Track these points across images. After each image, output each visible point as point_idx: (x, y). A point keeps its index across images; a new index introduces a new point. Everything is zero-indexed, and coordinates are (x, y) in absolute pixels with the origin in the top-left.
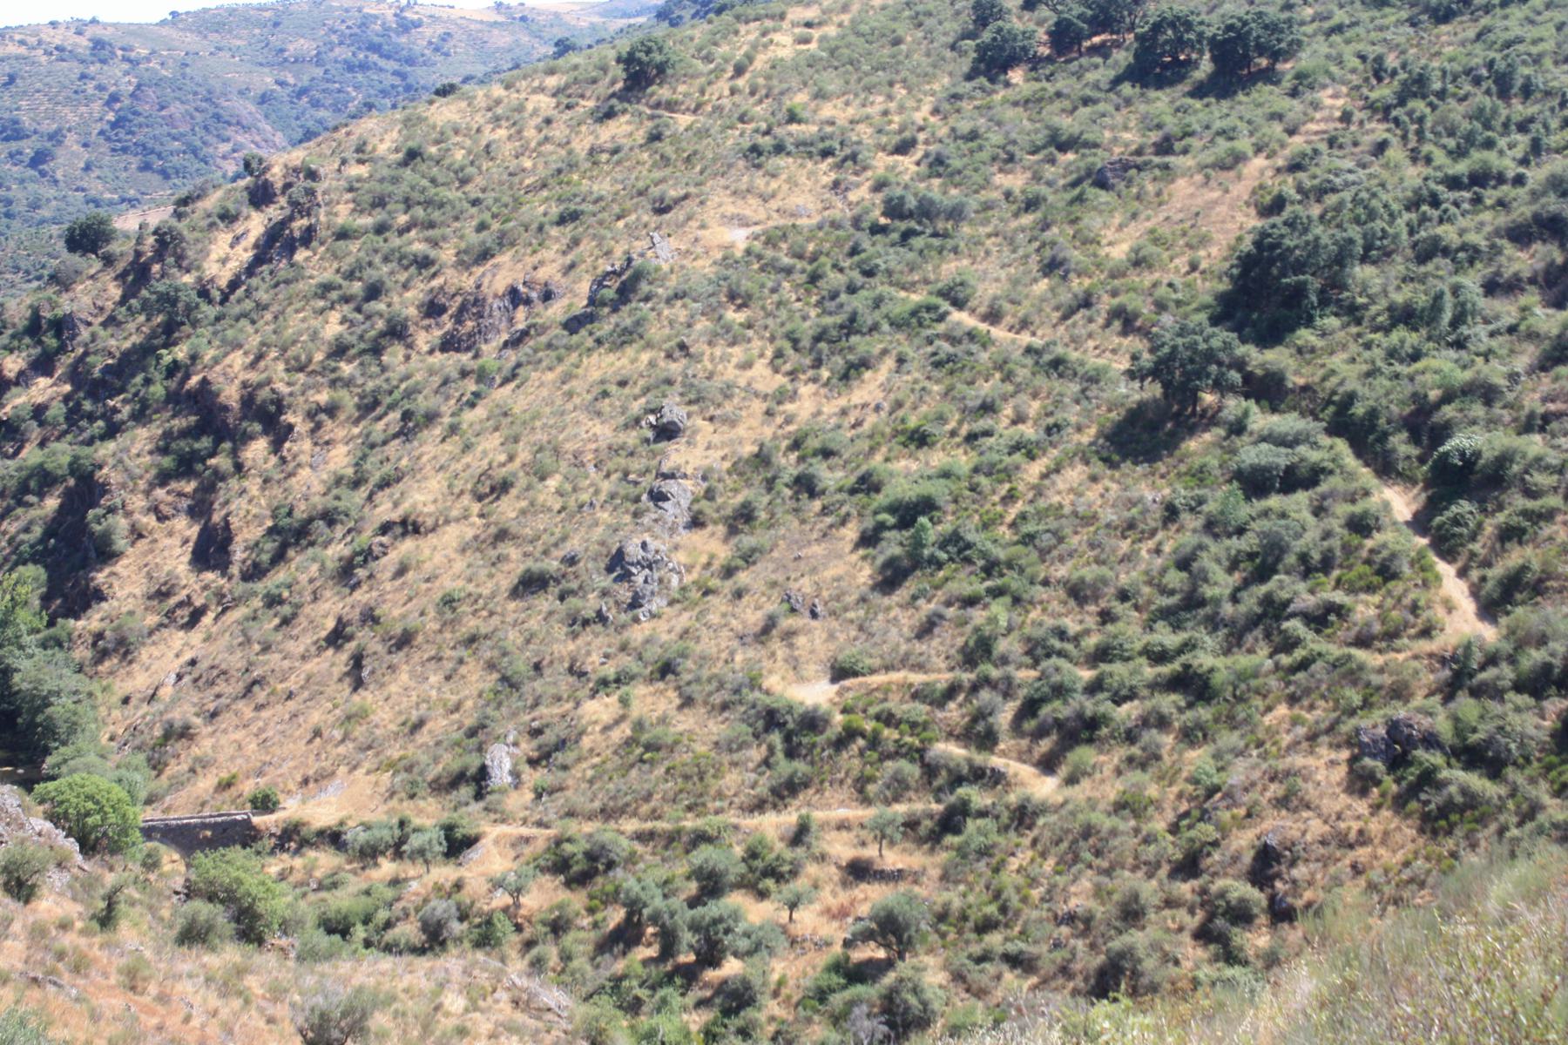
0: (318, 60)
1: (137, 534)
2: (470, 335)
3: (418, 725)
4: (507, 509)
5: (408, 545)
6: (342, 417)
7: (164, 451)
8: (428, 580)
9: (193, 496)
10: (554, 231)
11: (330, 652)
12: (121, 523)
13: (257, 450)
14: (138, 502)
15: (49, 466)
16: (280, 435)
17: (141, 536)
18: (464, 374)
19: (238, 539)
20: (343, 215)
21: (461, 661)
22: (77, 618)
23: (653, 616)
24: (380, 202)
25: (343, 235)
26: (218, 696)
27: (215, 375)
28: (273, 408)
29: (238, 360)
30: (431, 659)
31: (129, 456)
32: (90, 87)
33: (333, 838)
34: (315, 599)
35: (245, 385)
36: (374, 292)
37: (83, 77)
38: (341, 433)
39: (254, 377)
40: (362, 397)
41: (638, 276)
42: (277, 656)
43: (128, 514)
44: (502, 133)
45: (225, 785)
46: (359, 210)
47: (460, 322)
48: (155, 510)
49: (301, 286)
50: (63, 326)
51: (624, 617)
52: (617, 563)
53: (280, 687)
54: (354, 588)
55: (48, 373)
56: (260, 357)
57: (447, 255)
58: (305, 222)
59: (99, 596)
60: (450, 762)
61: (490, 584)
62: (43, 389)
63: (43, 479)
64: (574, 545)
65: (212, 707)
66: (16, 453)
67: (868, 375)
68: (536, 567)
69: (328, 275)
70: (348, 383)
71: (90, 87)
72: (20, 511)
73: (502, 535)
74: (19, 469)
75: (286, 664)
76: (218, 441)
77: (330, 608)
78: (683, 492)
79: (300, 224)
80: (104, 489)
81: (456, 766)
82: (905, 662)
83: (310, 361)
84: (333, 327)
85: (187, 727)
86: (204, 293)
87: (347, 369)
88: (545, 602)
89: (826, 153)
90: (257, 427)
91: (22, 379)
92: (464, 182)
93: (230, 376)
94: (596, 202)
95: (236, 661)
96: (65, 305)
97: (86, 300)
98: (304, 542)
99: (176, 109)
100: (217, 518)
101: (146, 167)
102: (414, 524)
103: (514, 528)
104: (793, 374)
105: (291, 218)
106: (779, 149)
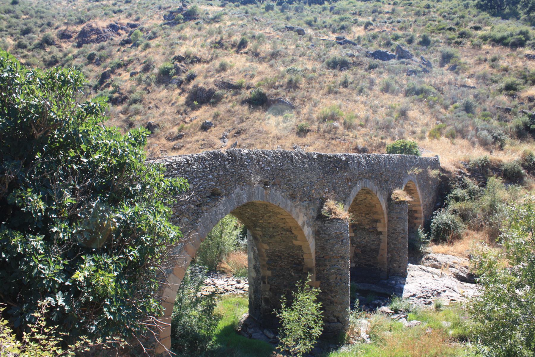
10: (114, 15)
11: (204, 108)
34: (149, 92)
40: (44, 61)
73: (274, 55)
87: (30, 53)
102: (196, 58)
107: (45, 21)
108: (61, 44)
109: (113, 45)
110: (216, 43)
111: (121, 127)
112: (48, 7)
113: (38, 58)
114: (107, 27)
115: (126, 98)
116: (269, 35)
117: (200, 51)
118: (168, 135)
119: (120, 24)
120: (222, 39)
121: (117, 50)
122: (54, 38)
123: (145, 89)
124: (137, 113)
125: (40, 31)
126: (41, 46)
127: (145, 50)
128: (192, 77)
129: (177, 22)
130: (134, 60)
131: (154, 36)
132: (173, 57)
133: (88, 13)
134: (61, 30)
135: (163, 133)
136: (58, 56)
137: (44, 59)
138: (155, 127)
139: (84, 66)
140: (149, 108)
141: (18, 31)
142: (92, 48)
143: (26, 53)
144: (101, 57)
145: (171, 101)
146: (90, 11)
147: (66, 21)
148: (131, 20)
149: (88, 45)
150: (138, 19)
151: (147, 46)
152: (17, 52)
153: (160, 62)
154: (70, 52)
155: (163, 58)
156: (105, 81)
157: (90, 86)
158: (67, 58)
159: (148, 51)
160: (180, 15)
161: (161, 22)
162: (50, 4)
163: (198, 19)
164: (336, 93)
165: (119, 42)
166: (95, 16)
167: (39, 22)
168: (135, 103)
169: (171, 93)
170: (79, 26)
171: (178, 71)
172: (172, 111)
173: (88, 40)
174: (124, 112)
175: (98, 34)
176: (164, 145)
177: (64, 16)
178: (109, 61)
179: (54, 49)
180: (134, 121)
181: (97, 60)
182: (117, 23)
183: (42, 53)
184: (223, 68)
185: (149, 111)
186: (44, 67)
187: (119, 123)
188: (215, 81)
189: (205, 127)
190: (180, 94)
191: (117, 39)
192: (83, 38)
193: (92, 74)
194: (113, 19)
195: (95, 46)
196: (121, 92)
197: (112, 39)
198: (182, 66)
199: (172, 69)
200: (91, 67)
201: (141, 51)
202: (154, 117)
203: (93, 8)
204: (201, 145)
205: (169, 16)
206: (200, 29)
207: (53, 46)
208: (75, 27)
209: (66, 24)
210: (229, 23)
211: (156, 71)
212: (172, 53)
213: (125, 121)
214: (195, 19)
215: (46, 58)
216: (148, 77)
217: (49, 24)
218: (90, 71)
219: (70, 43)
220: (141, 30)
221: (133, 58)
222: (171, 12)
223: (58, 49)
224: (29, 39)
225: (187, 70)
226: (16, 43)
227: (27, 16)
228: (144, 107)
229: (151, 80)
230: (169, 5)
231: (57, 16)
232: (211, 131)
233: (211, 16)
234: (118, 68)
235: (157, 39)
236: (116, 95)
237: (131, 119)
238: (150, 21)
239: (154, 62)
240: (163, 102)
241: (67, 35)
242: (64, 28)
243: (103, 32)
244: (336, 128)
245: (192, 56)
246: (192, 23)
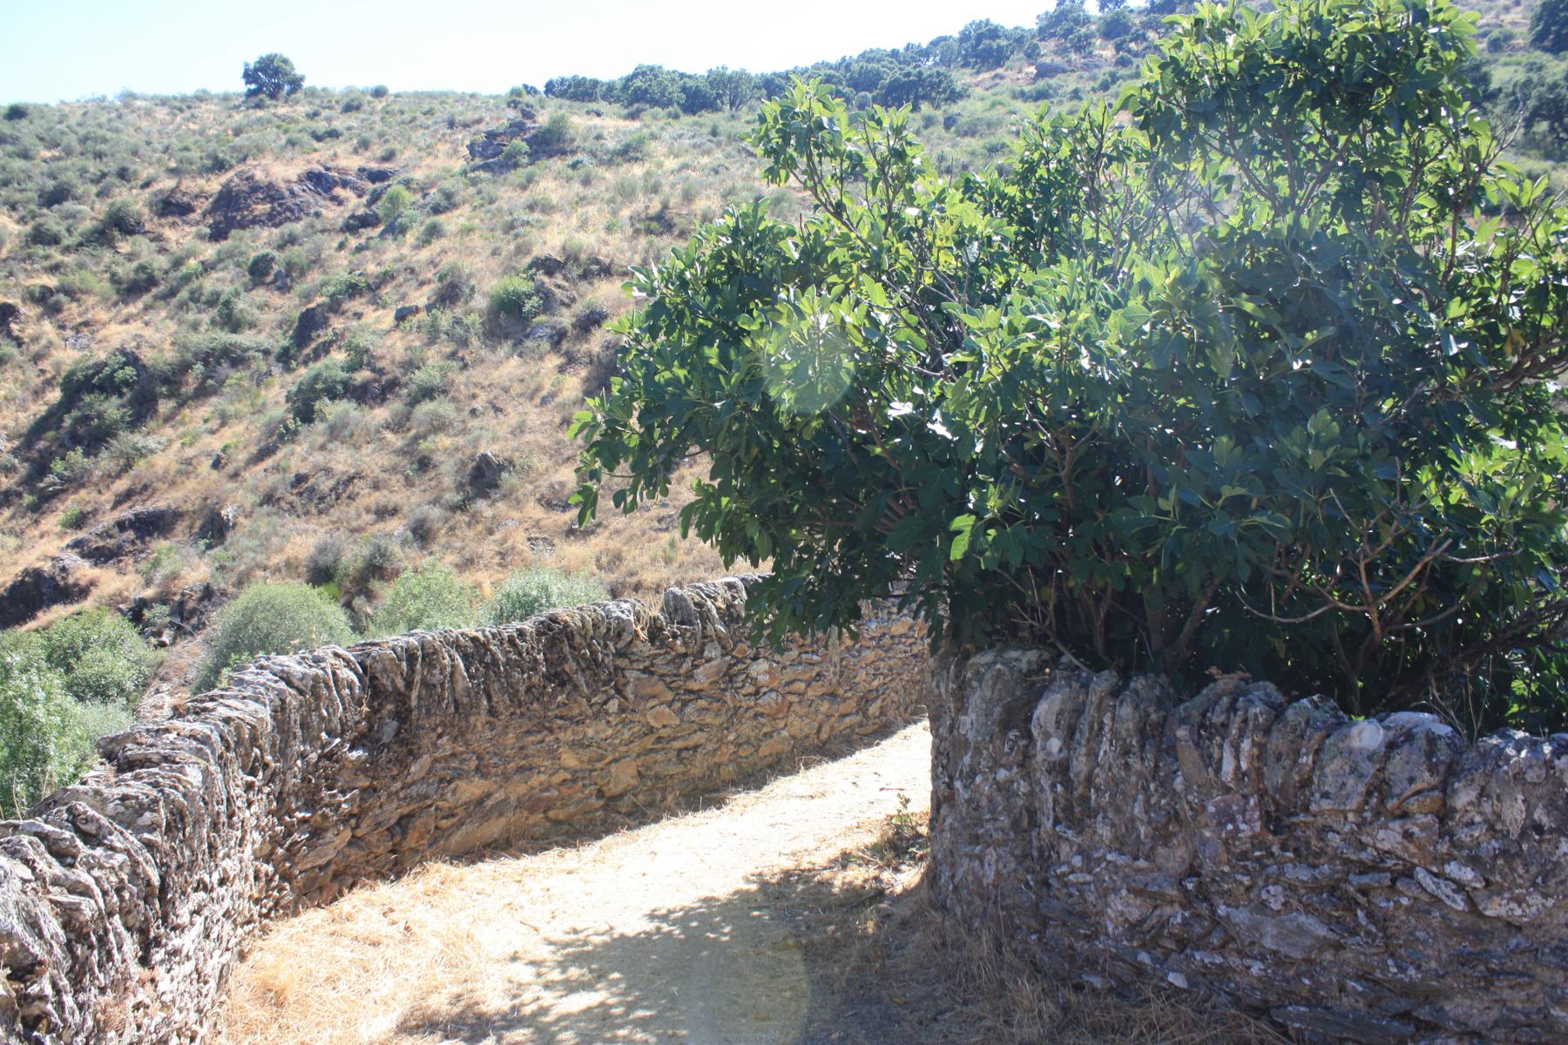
10: (316, 145)
34: (465, 367)
38: (103, 315)
40: (114, 279)
87: (69, 259)
102: (597, 262)
107: (111, 166)
108: (161, 230)
109: (323, 231)
110: (651, 219)
111: (394, 470)
112: (117, 124)
113: (95, 274)
114: (300, 181)
115: (393, 384)
118: (544, 490)
119: (338, 170)
120: (665, 207)
121: (335, 245)
122: (140, 214)
123: (453, 355)
124: (439, 426)
125: (99, 195)
127: (429, 242)
128: (591, 321)
129: (510, 163)
130: (398, 271)
131: (448, 203)
132: (528, 260)
133: (238, 141)
134: (161, 191)
135: (530, 487)
136: (155, 265)
137: (114, 275)
138: (501, 468)
139: (243, 294)
140: (473, 412)
141: (30, 194)
142: (258, 241)
143: (57, 256)
144: (290, 266)
145: (538, 389)
146: (244, 136)
147: (173, 164)
148: (369, 160)
149: (247, 234)
150: (389, 156)
151: (434, 232)
152: (30, 256)
153: (489, 281)
154: (191, 254)
155: (494, 263)
156: (314, 335)
157: (266, 352)
158: (184, 270)
159: (437, 245)
160: (519, 143)
161: (459, 165)
162: (120, 117)
163: (573, 152)
165: (340, 222)
166: (260, 150)
167: (93, 167)
168: (432, 399)
169: (533, 368)
170: (213, 177)
171: (548, 302)
172: (546, 419)
173: (243, 217)
174: (397, 425)
175: (272, 199)
176: (538, 522)
177: (166, 150)
178: (314, 277)
179: (143, 245)
180: (432, 451)
181: (278, 274)
182: (328, 169)
183: (107, 256)
185: (476, 423)
186: (115, 297)
187: (386, 460)
190: (561, 369)
191: (334, 215)
192: (229, 213)
193: (268, 317)
194: (316, 156)
196: (380, 364)
197: (317, 215)
198: (559, 287)
199: (529, 296)
200: (260, 294)
201: (417, 247)
202: (495, 440)
203: (250, 125)
204: (660, 520)
205: (485, 146)
206: (586, 182)
207: (138, 237)
208: (201, 182)
209: (173, 172)
210: (671, 164)
211: (480, 302)
212: (521, 250)
213: (402, 452)
214: (564, 153)
215: (120, 271)
216: (458, 322)
217: (123, 174)
218: (261, 308)
219: (187, 229)
220: (407, 184)
221: (398, 266)
222: (491, 135)
223: (153, 245)
225: (573, 300)
226: (28, 228)
228: (459, 410)
229: (467, 331)
230: (476, 116)
231: (144, 150)
232: (683, 477)
233: (611, 144)
234: (352, 296)
235: (457, 212)
236: (363, 375)
237: (423, 445)
238: (429, 160)
239: (470, 276)
240: (513, 393)
241: (178, 205)
242: (167, 183)
243: (287, 194)
245: (583, 257)
246: (557, 164)
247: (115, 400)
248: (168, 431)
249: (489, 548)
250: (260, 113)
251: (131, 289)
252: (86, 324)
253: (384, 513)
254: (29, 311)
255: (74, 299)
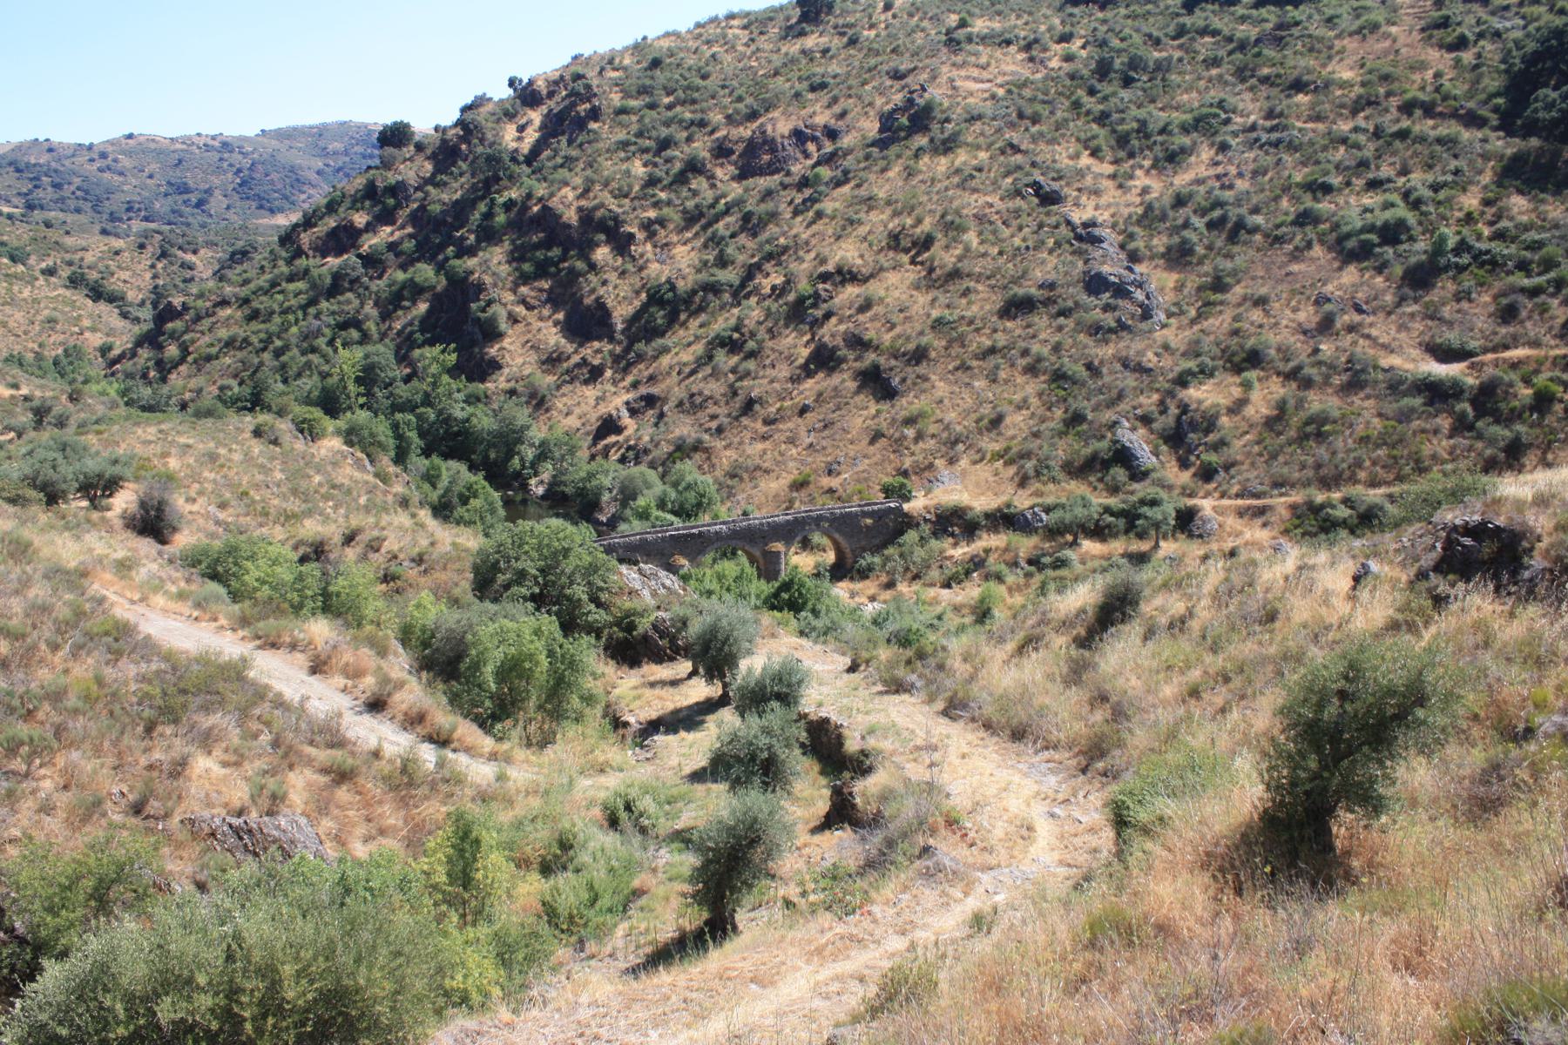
0: (346, 153)
1: (514, 319)
2: (770, 164)
3: (996, 422)
4: (944, 257)
5: (851, 291)
6: (672, 226)
7: (522, 259)
8: (901, 311)
9: (550, 291)
10: (810, 96)
11: (821, 375)
12: (502, 314)
13: (602, 253)
14: (509, 297)
15: (417, 280)
16: (622, 244)
17: (516, 321)
18: (785, 187)
19: (615, 314)
20: (616, 99)
21: (997, 367)
22: (483, 381)
23: (1164, 326)
24: (643, 91)
25: (623, 111)
26: (713, 417)
27: (554, 203)
28: (611, 223)
29: (569, 193)
30: (957, 369)
31: (492, 264)
32: (225, 165)
33: (1005, 520)
34: (773, 337)
35: (580, 209)
36: (665, 144)
37: (221, 159)
38: (675, 239)
39: (583, 203)
40: (685, 212)
41: (928, 109)
42: (766, 381)
43: (505, 305)
44: (715, 49)
45: (799, 485)
46: (627, 95)
47: (755, 158)
48: (523, 302)
49: (601, 145)
50: (397, 190)
51: (1144, 326)
52: (1095, 284)
53: (788, 403)
54: (816, 323)
55: (393, 223)
56: (587, 191)
57: (717, 117)
58: (588, 106)
59: (495, 366)
60: (1063, 450)
61: (975, 308)
62: (386, 234)
63: (415, 290)
64: (1038, 275)
65: (714, 425)
66: (380, 277)
67: (1193, 159)
68: (1020, 291)
69: (621, 135)
70: (669, 203)
71: (225, 165)
72: (400, 313)
73: (955, 274)
74: (390, 286)
75: (776, 385)
76: (566, 251)
77: (797, 344)
78: (1111, 237)
79: (583, 108)
80: (480, 288)
81: (1088, 451)
82: (1514, 342)
83: (630, 187)
84: (639, 169)
85: (700, 441)
86: (514, 159)
88: (1041, 321)
89: (1008, 43)
90: (603, 237)
91: (370, 228)
92: (704, 77)
93: (567, 203)
94: (835, 77)
95: (715, 388)
96: (392, 178)
97: (412, 174)
98: (694, 307)
99: (274, 176)
100: (588, 301)
101: (261, 207)
102: (850, 272)
103: (965, 266)
104: (1116, 162)
105: (573, 105)
106: (970, 39)
111: (724, 395)
116: (987, 211)
117: (862, 256)
124: (748, 374)
126: (681, 179)
128: (828, 315)
150: (843, 115)
160: (904, 121)
164: (969, 368)
174: (734, 371)
184: (866, 306)
188: (845, 333)
189: (803, 410)
191: (798, 169)
193: (741, 258)
194: (803, 112)
195: (764, 182)
197: (788, 174)
200: (743, 239)
211: (791, 297)
213: (731, 386)
217: (702, 124)
224: (667, 161)
227: (671, 99)
237: (738, 384)
244: (905, 438)
247: (662, 313)
248: (681, 332)
249: (737, 440)
250: (793, 47)
251: (691, 218)
252: (666, 245)
253: (713, 417)
254: (640, 236)
255: (663, 227)
